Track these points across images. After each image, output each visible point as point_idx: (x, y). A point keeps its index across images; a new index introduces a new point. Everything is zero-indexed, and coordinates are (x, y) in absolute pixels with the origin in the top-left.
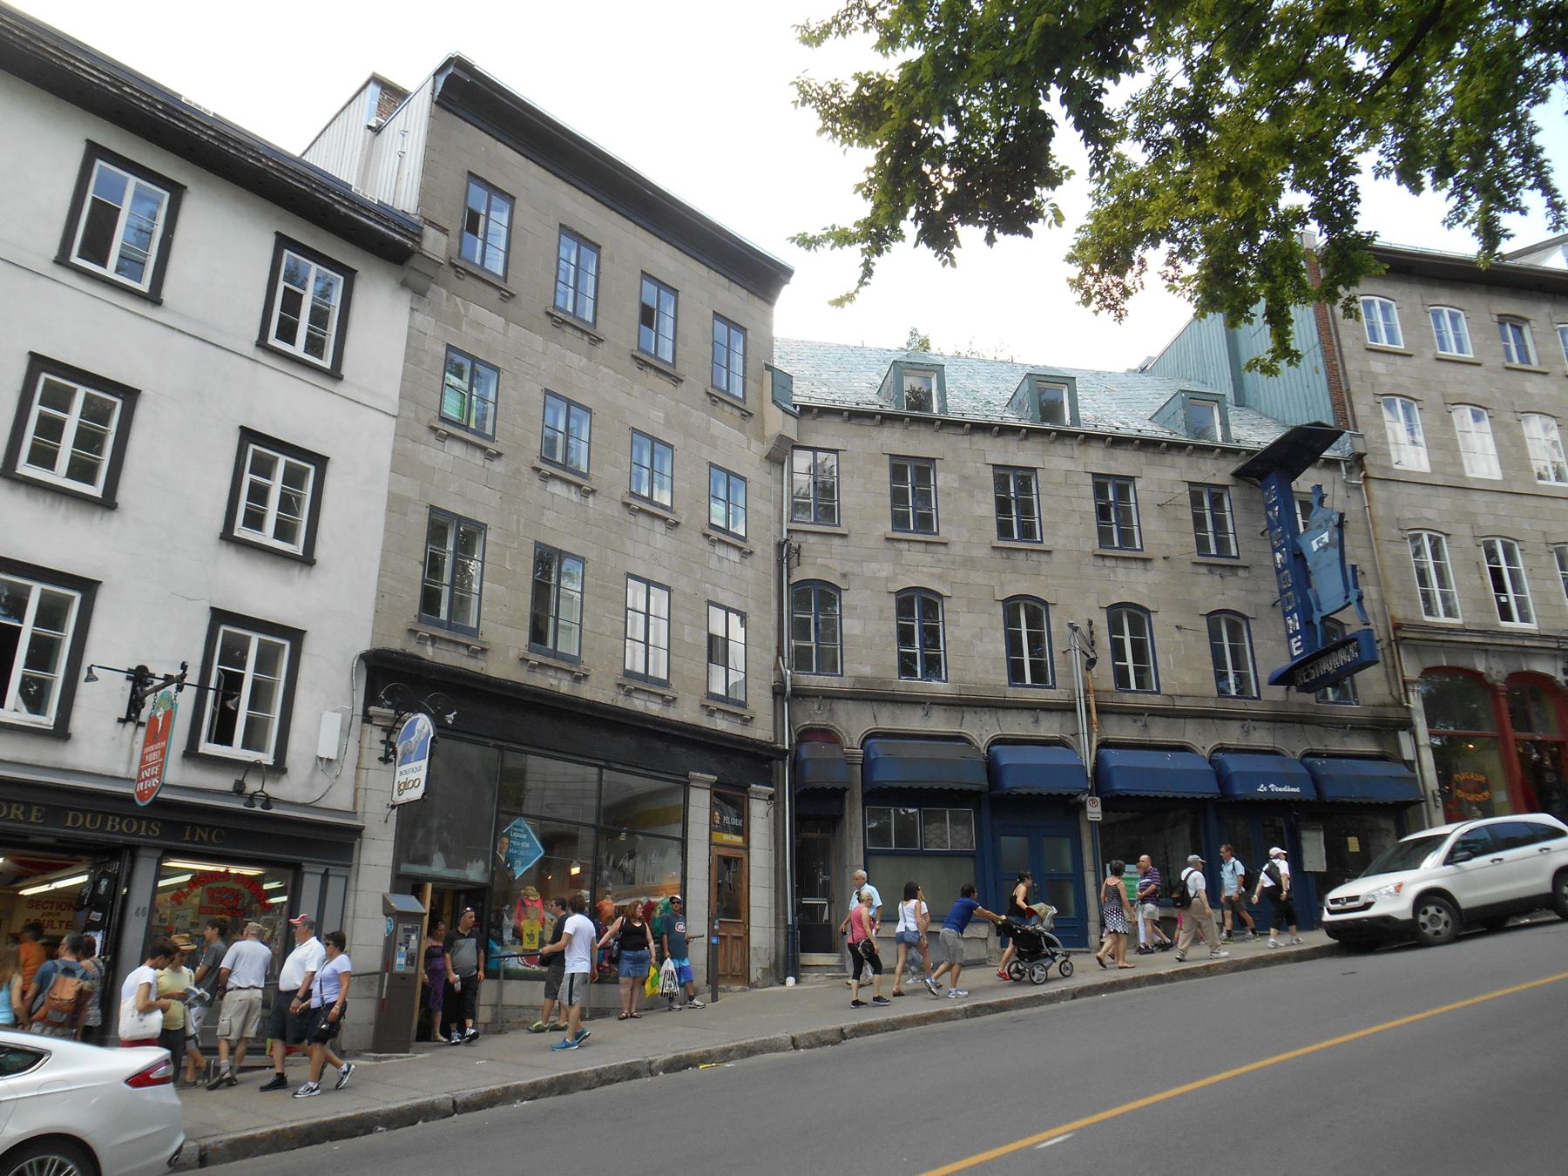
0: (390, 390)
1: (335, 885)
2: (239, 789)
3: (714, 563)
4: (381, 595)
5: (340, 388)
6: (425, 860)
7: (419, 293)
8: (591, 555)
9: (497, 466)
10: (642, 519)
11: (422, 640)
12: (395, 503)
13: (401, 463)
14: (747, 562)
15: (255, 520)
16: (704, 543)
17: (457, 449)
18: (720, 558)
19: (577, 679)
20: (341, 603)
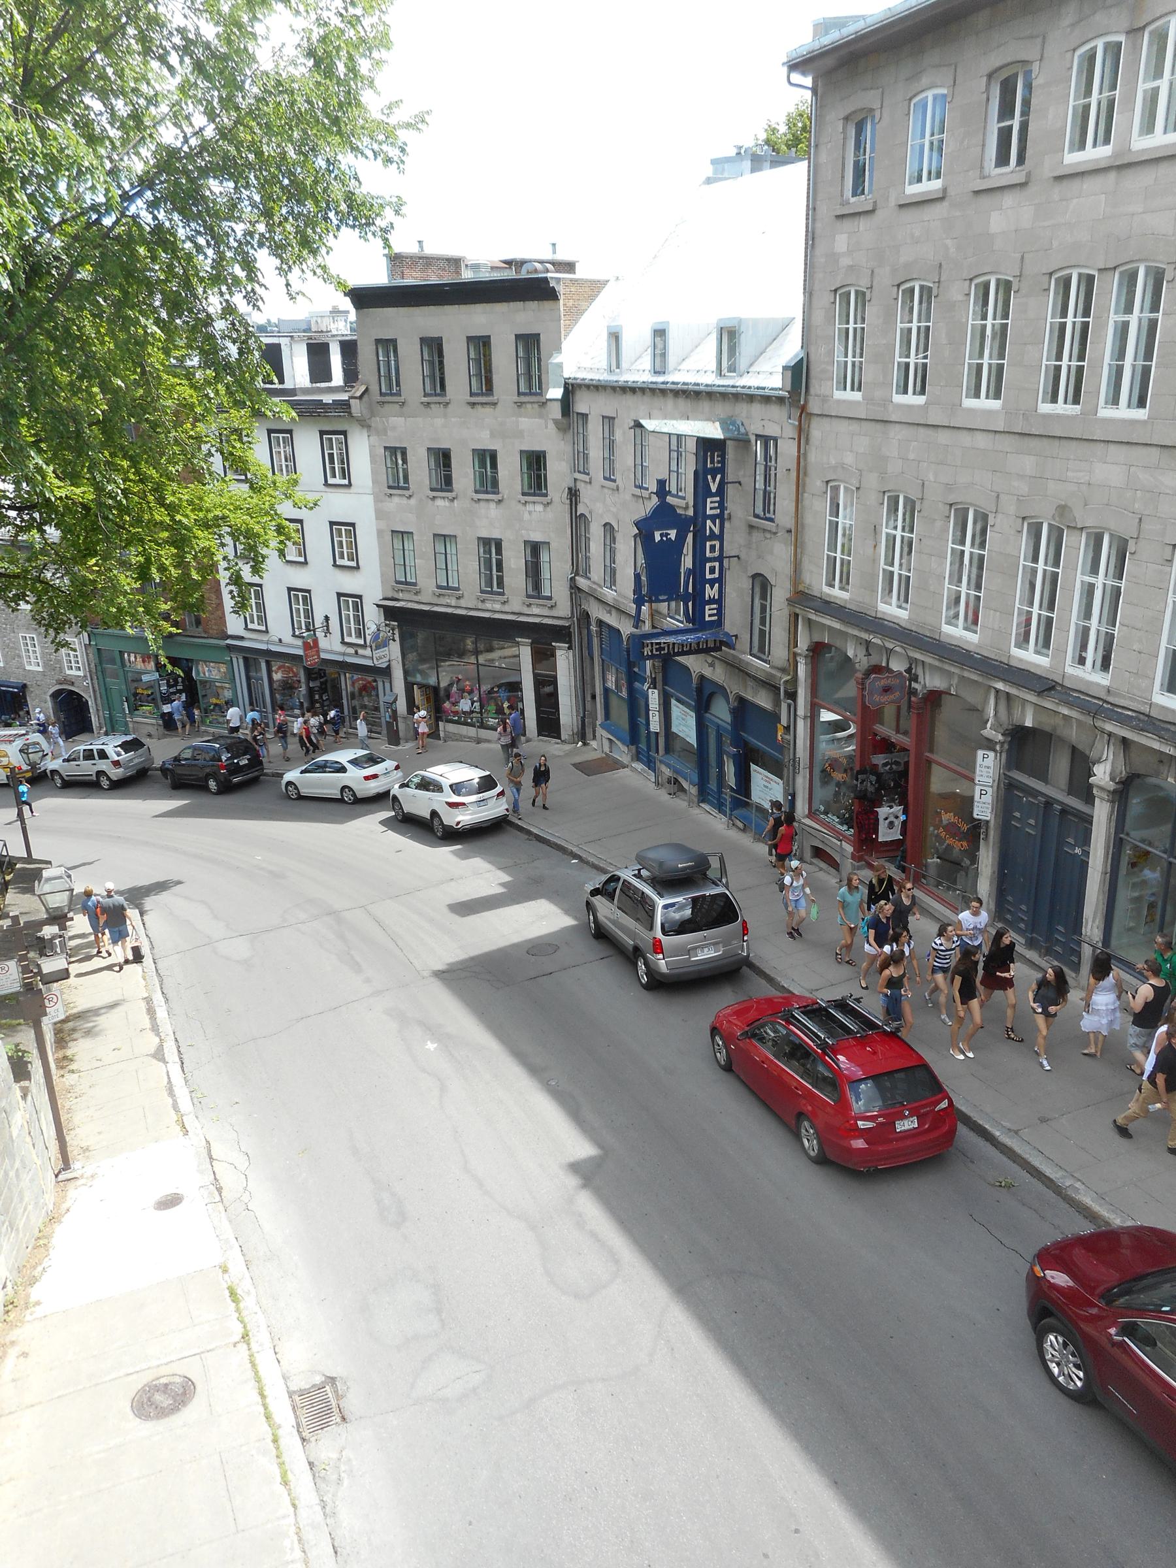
0: (369, 482)
1: (387, 685)
2: (356, 653)
3: (526, 516)
4: (382, 575)
5: (353, 489)
6: (415, 676)
7: (369, 427)
8: (458, 533)
9: (413, 501)
10: (482, 504)
11: (397, 591)
12: (380, 533)
13: (380, 515)
14: (548, 509)
15: (342, 557)
16: (520, 507)
17: (396, 500)
18: (530, 512)
19: (458, 598)
20: (370, 584)
